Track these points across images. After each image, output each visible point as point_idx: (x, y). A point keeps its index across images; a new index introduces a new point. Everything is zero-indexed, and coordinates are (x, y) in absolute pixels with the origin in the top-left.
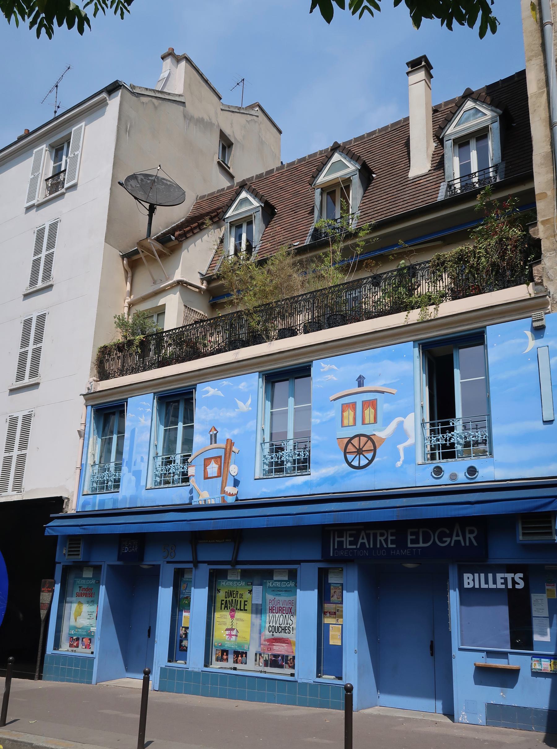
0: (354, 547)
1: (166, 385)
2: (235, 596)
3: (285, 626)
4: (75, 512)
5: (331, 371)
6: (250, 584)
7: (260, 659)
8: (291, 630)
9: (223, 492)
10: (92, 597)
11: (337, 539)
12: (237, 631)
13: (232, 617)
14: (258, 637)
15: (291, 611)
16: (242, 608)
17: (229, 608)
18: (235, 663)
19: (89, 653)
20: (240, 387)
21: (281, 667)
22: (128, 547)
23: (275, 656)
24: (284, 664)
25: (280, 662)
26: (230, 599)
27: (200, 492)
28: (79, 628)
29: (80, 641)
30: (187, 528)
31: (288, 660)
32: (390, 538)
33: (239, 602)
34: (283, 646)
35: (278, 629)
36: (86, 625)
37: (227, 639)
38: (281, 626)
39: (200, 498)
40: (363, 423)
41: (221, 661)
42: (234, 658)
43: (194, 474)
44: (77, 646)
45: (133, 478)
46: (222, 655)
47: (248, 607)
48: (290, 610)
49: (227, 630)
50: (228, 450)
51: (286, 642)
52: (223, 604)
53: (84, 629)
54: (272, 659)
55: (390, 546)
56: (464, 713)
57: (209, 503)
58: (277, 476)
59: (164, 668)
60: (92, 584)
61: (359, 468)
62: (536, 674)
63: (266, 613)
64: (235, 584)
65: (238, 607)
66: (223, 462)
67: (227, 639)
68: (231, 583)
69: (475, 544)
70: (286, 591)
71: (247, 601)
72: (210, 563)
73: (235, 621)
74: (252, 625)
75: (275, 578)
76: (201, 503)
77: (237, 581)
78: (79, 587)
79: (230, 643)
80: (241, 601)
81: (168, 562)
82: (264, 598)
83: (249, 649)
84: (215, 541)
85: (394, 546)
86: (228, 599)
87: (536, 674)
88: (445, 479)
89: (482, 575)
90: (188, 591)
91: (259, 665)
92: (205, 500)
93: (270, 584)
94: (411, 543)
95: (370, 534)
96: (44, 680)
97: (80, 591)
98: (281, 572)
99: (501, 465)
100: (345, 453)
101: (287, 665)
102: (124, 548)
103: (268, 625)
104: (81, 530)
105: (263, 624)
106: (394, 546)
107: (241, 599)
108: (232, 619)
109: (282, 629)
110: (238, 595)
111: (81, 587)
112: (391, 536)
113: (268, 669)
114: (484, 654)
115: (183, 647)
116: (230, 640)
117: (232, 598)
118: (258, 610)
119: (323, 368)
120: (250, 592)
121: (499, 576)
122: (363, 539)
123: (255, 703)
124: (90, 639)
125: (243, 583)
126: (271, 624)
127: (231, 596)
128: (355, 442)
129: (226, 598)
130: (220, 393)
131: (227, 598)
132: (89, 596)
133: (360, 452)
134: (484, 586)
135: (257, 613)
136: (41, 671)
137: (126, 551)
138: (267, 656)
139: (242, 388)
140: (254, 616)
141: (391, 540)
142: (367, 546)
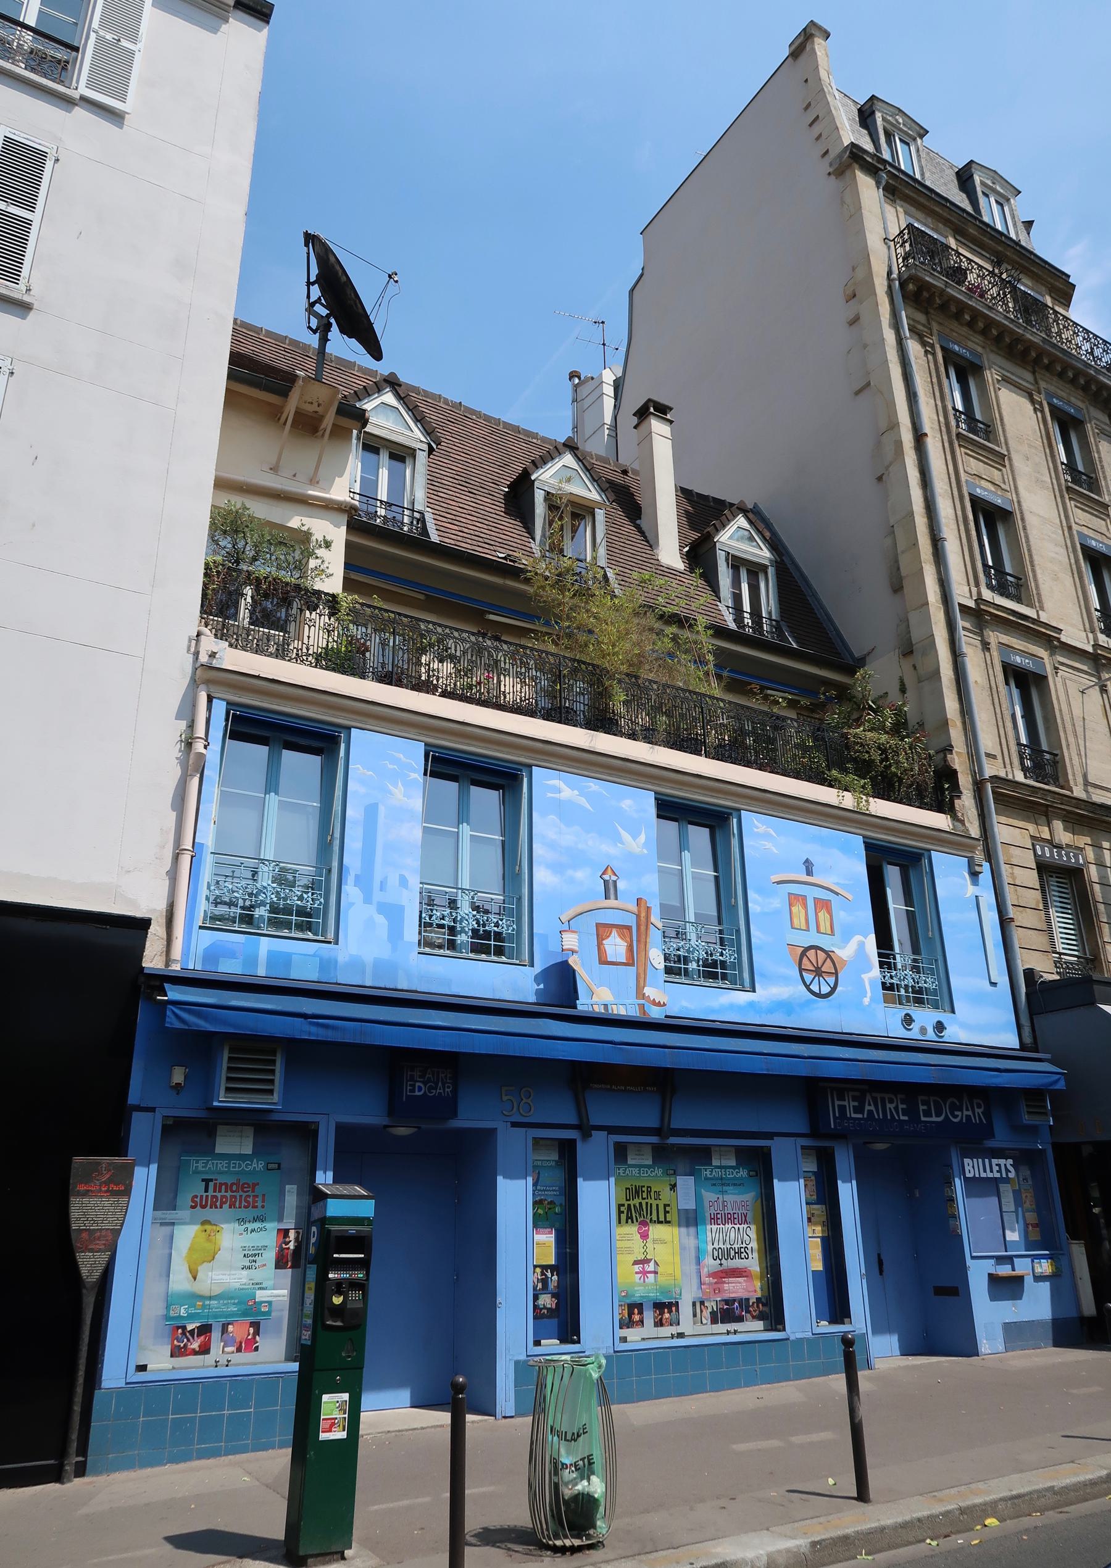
0: (860, 1116)
1: (497, 748)
2: (645, 1195)
3: (739, 1246)
4: (179, 968)
5: (766, 836)
6: (672, 1172)
7: (701, 1311)
8: (749, 1252)
9: (641, 996)
10: (255, 1207)
11: (837, 1103)
12: (656, 1263)
13: (644, 1236)
14: (695, 1271)
15: (746, 1220)
16: (662, 1218)
17: (635, 1221)
18: (658, 1327)
19: (280, 1362)
20: (624, 806)
21: (740, 1319)
22: (425, 1084)
23: (727, 1302)
24: (744, 1313)
25: (737, 1312)
26: (636, 1201)
27: (594, 988)
28: (210, 1298)
29: (216, 1335)
30: (802, 1069)
31: (750, 1306)
32: (901, 1106)
33: (654, 1207)
34: (740, 1283)
35: (729, 1254)
36: (237, 1286)
37: (638, 1281)
38: (733, 1247)
39: (595, 999)
40: (818, 931)
41: (628, 1328)
42: (655, 1318)
43: (576, 948)
44: (205, 1350)
45: (381, 920)
46: (631, 1314)
47: (673, 1216)
48: (745, 1217)
49: (636, 1263)
50: (643, 919)
51: (744, 1274)
52: (623, 1212)
53: (232, 1298)
54: (723, 1309)
55: (902, 1118)
56: (985, 1341)
57: (615, 1012)
58: (708, 984)
59: (525, 1362)
60: (253, 1172)
61: (819, 995)
62: (1038, 1278)
63: (705, 1224)
64: (643, 1173)
65: (655, 1218)
66: (635, 938)
67: (638, 1281)
68: (635, 1171)
69: (964, 1121)
70: (735, 1185)
71: (669, 1205)
72: (611, 1130)
73: (650, 1245)
74: (683, 1248)
75: (715, 1162)
76: (597, 1009)
77: (648, 1167)
78: (203, 1180)
79: (644, 1288)
80: (657, 1205)
81: (514, 1125)
82: (698, 1198)
83: (681, 1295)
84: (625, 1088)
85: (906, 1118)
86: (631, 1203)
87: (1038, 1278)
88: (914, 1033)
89: (980, 1160)
90: (542, 1188)
91: (702, 1323)
92: (606, 1006)
93: (707, 1172)
94: (924, 1116)
95: (876, 1098)
96: (97, 1473)
97: (206, 1190)
98: (723, 1150)
99: (963, 1026)
100: (801, 970)
101: (748, 1315)
102: (414, 1086)
103: (710, 1247)
104: (313, 1029)
105: (702, 1246)
106: (906, 1118)
107: (658, 1202)
108: (645, 1242)
109: (735, 1253)
110: (652, 1194)
111: (211, 1180)
112: (902, 1103)
113: (722, 1328)
114: (992, 1261)
115: (541, 1309)
116: (644, 1282)
117: (641, 1200)
118: (691, 1219)
119: (757, 828)
120: (673, 1187)
121: (995, 1161)
122: (870, 1105)
123: (708, 1394)
124: (256, 1326)
125: (659, 1172)
126: (716, 1245)
127: (638, 1197)
128: (811, 954)
129: (627, 1200)
130: (583, 801)
131: (629, 1200)
132: (243, 1203)
133: (818, 972)
134: (983, 1175)
135: (688, 1225)
136: (83, 1450)
137: (417, 1093)
138: (714, 1304)
139: (627, 808)
140: (684, 1230)
141: (902, 1109)
142: (876, 1117)
